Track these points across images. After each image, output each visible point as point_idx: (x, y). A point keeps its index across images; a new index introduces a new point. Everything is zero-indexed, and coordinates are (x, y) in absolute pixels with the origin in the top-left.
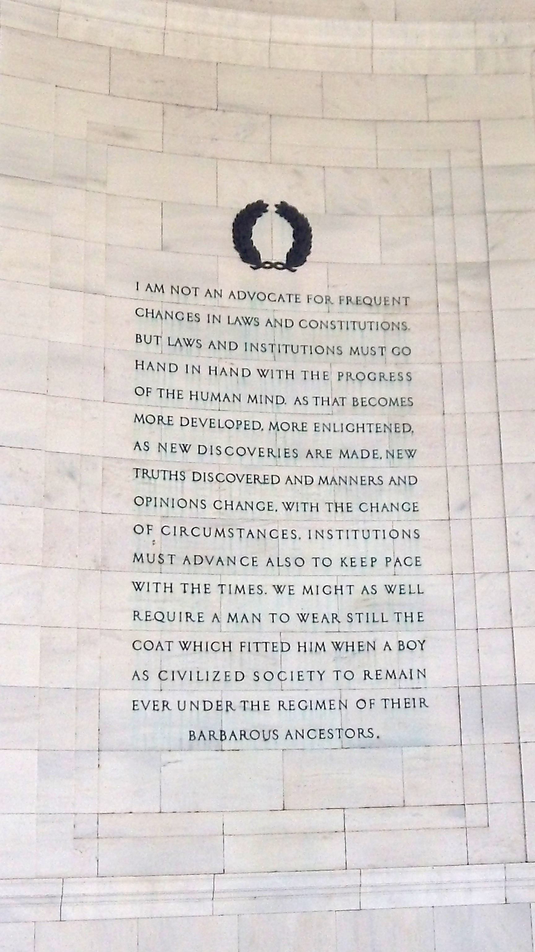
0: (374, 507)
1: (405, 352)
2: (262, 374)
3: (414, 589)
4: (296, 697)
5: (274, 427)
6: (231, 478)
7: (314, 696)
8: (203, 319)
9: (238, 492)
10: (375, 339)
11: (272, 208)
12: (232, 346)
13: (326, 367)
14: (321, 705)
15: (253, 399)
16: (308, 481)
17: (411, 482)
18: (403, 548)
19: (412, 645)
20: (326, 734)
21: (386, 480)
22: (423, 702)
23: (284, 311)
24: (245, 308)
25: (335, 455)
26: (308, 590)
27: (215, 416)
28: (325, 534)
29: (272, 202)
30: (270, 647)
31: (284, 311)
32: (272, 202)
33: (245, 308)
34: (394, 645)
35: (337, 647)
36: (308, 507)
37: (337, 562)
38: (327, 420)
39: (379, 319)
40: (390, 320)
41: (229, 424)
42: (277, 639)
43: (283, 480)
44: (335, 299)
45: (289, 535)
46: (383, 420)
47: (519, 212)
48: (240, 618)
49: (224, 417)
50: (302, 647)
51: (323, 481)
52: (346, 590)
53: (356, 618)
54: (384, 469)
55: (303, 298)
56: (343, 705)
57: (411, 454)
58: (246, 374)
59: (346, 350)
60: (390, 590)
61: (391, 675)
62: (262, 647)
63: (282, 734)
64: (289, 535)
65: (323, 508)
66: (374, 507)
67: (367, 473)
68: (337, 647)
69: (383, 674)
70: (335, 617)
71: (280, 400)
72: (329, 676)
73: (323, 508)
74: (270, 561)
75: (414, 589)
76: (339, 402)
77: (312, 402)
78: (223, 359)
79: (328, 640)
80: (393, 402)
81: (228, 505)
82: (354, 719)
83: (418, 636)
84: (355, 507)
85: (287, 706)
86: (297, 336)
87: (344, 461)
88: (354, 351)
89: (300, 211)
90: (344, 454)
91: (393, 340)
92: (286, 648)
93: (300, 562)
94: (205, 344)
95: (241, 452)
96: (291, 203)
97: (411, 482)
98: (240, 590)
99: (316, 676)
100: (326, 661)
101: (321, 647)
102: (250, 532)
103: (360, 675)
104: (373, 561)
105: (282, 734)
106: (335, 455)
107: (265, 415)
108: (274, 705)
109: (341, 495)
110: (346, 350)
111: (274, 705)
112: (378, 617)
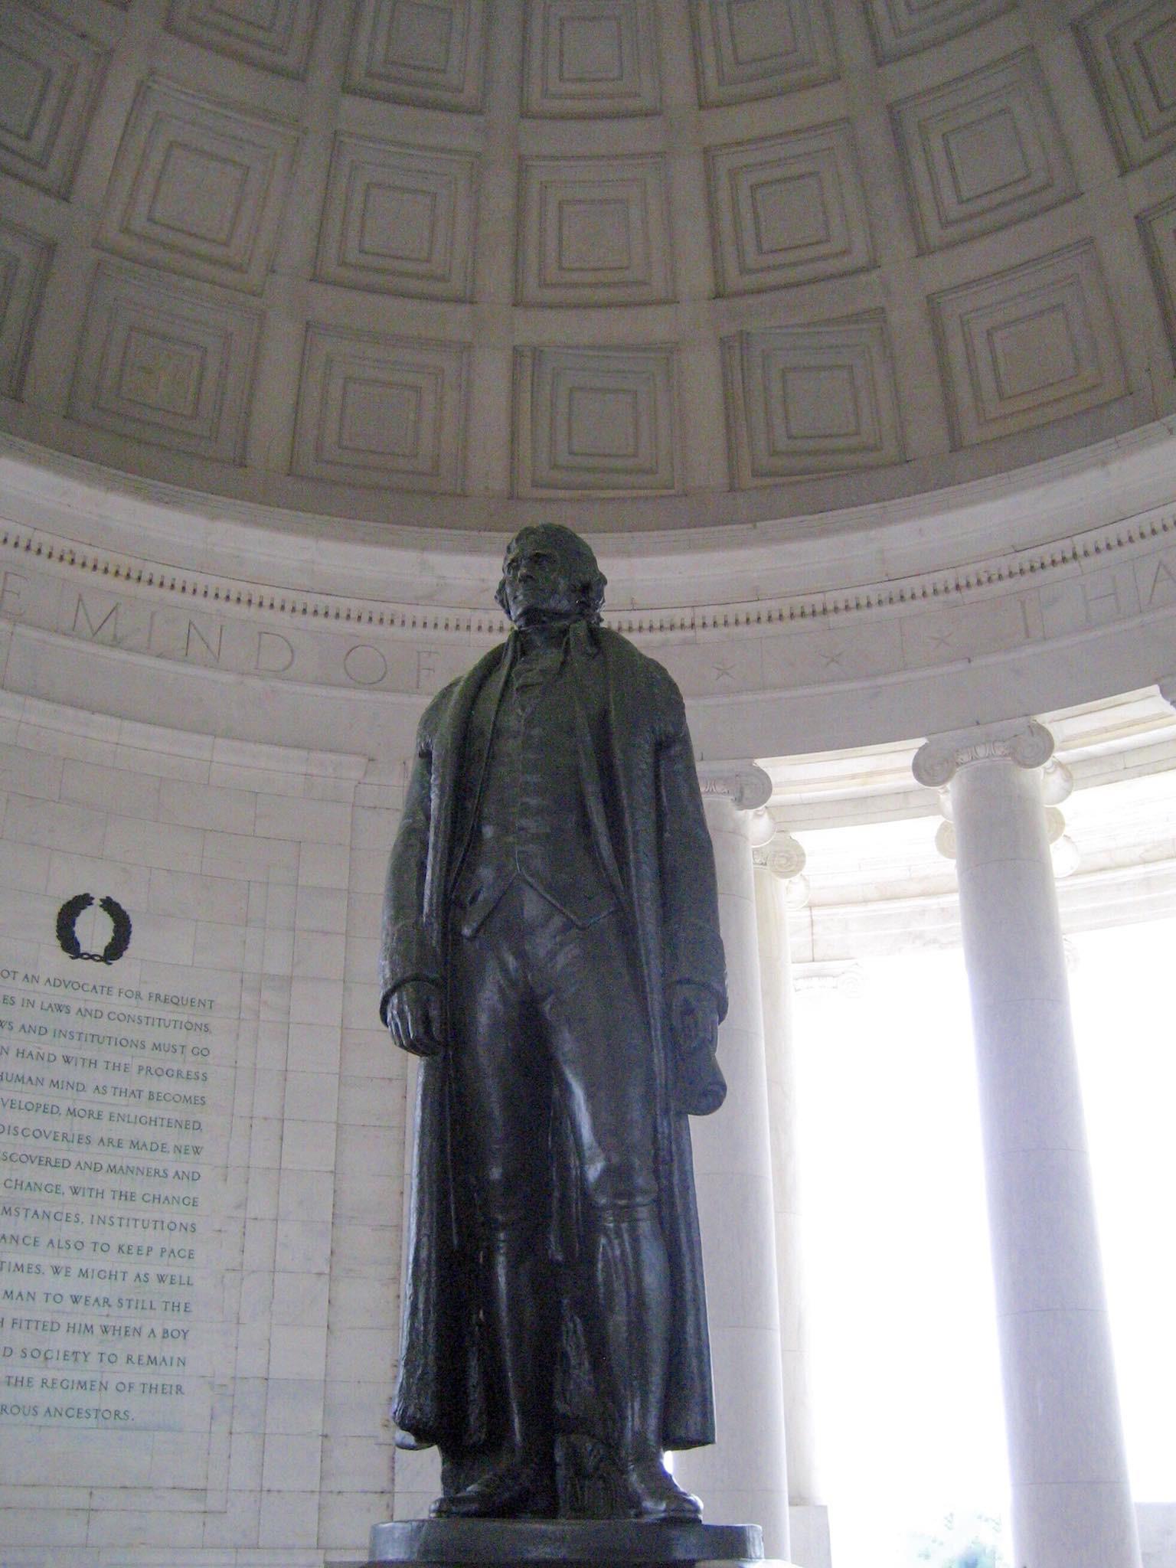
0: (157, 1199)
1: (204, 1052)
2: (67, 1060)
3: (185, 1280)
4: (59, 1376)
5: (72, 1112)
6: (24, 1158)
7: (78, 1376)
8: (18, 1002)
9: (29, 1173)
10: (178, 1037)
11: (97, 902)
12: (43, 1031)
13: (128, 1060)
14: (82, 1385)
15: (55, 1084)
16: (96, 1168)
17: (194, 1177)
18: (179, 1240)
19: (175, 1334)
20: (84, 1414)
21: (171, 1174)
22: (179, 1389)
23: (95, 1002)
24: (59, 995)
25: (126, 1144)
26: (84, 1274)
27: (17, 1097)
28: (108, 1221)
29: (98, 896)
30: (40, 1326)
31: (95, 1002)
32: (98, 896)
33: (59, 995)
34: (159, 1332)
35: (105, 1330)
36: (94, 1194)
37: (114, 1248)
38: (124, 1111)
39: (185, 1018)
40: (194, 1020)
41: (29, 1106)
42: (48, 1319)
43: (74, 1165)
44: (144, 994)
45: (73, 1218)
46: (175, 1116)
47: (326, 933)
48: (15, 1294)
49: (25, 1098)
50: (71, 1328)
51: (112, 1169)
52: (120, 1276)
53: (125, 1303)
54: (168, 1161)
55: (115, 991)
56: (104, 1387)
57: (197, 1151)
58: (52, 1059)
59: (149, 1045)
60: (161, 1279)
61: (152, 1360)
62: (33, 1325)
63: (42, 1410)
64: (73, 1218)
65: (108, 1195)
66: (157, 1199)
67: (154, 1165)
68: (105, 1330)
69: (145, 1360)
70: (106, 1301)
71: (81, 1087)
72: (94, 1358)
73: (108, 1195)
74: (51, 1242)
75: (185, 1280)
76: (137, 1094)
77: (110, 1091)
78: (31, 1042)
79: (97, 1323)
80: (187, 1100)
81: (19, 1184)
82: (110, 1401)
83: (180, 1326)
84: (138, 1198)
85: (49, 1383)
86: (103, 1027)
87: (134, 1152)
88: (156, 1047)
89: (123, 907)
90: (134, 1145)
91: (194, 1039)
92: (56, 1327)
93: (79, 1246)
94: (17, 1026)
95: (37, 1134)
96: (115, 899)
97: (194, 1177)
98: (19, 1268)
99: (81, 1357)
100: (91, 1344)
101: (89, 1329)
102: (36, 1213)
103: (122, 1359)
104: (150, 1249)
105: (42, 1410)
106: (126, 1144)
107: (65, 1100)
108: (37, 1382)
109: (127, 1184)
110: (149, 1045)
111: (37, 1382)
112: (147, 1305)
